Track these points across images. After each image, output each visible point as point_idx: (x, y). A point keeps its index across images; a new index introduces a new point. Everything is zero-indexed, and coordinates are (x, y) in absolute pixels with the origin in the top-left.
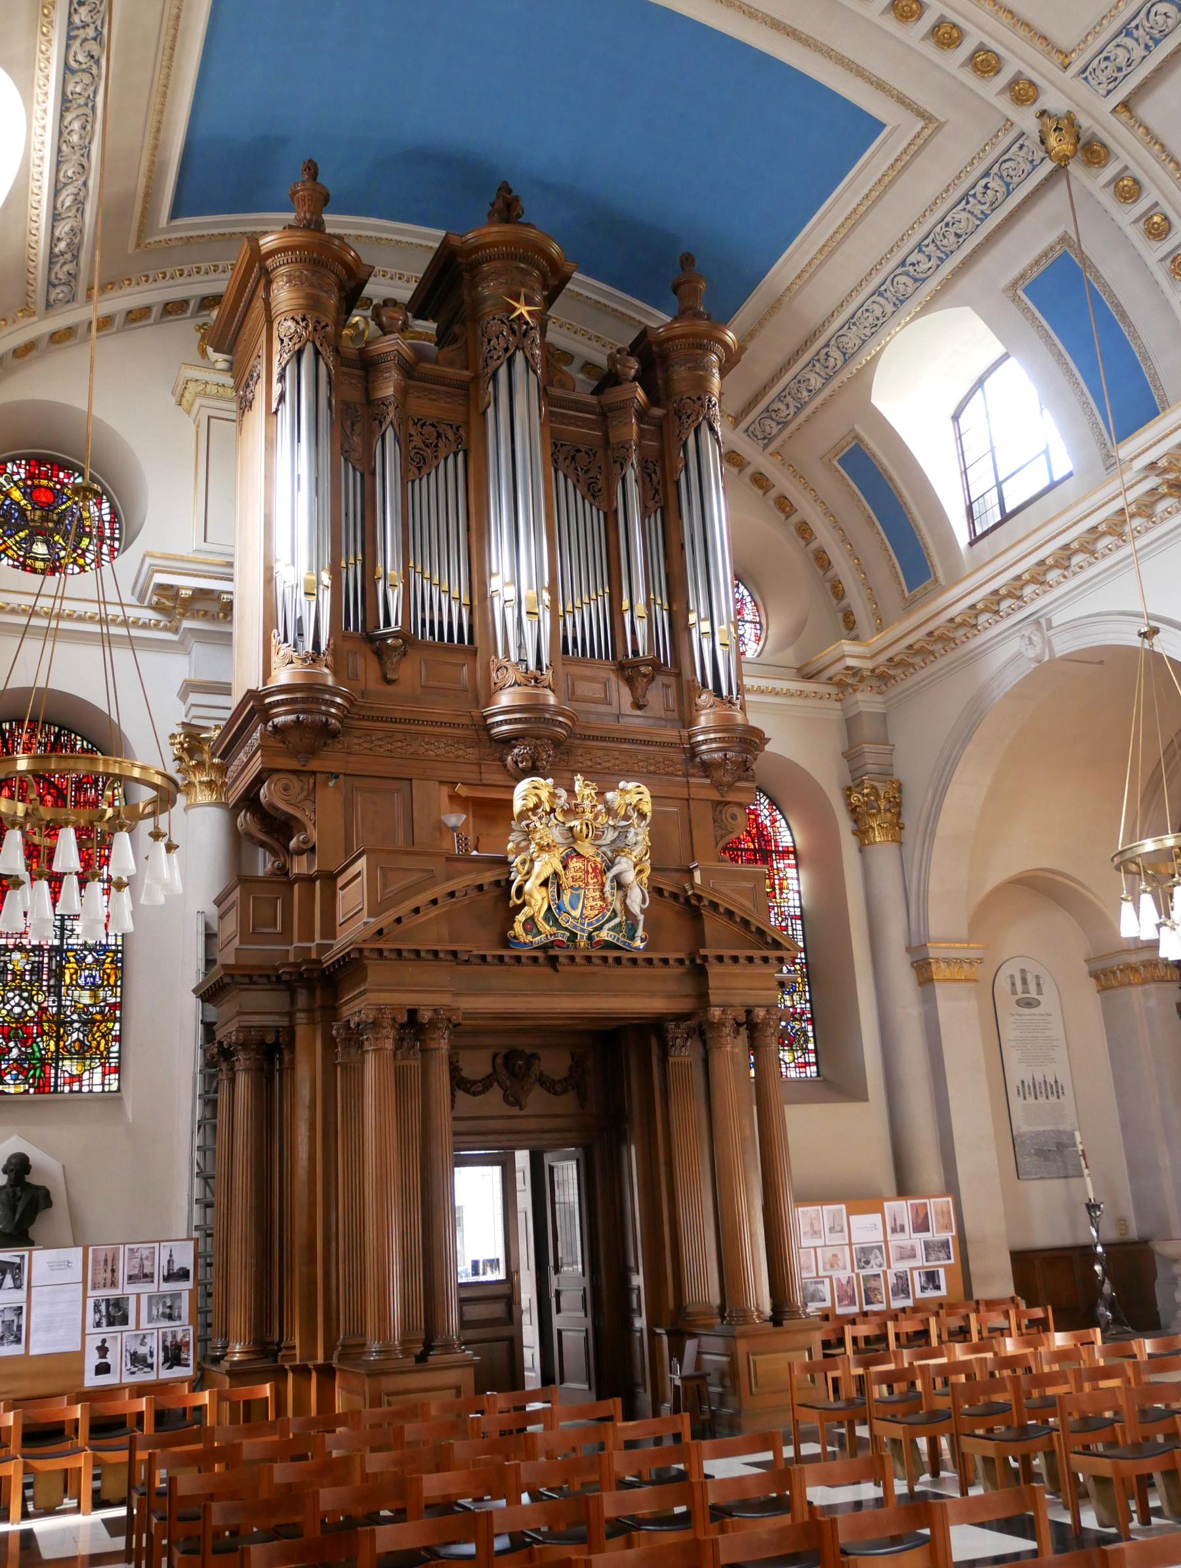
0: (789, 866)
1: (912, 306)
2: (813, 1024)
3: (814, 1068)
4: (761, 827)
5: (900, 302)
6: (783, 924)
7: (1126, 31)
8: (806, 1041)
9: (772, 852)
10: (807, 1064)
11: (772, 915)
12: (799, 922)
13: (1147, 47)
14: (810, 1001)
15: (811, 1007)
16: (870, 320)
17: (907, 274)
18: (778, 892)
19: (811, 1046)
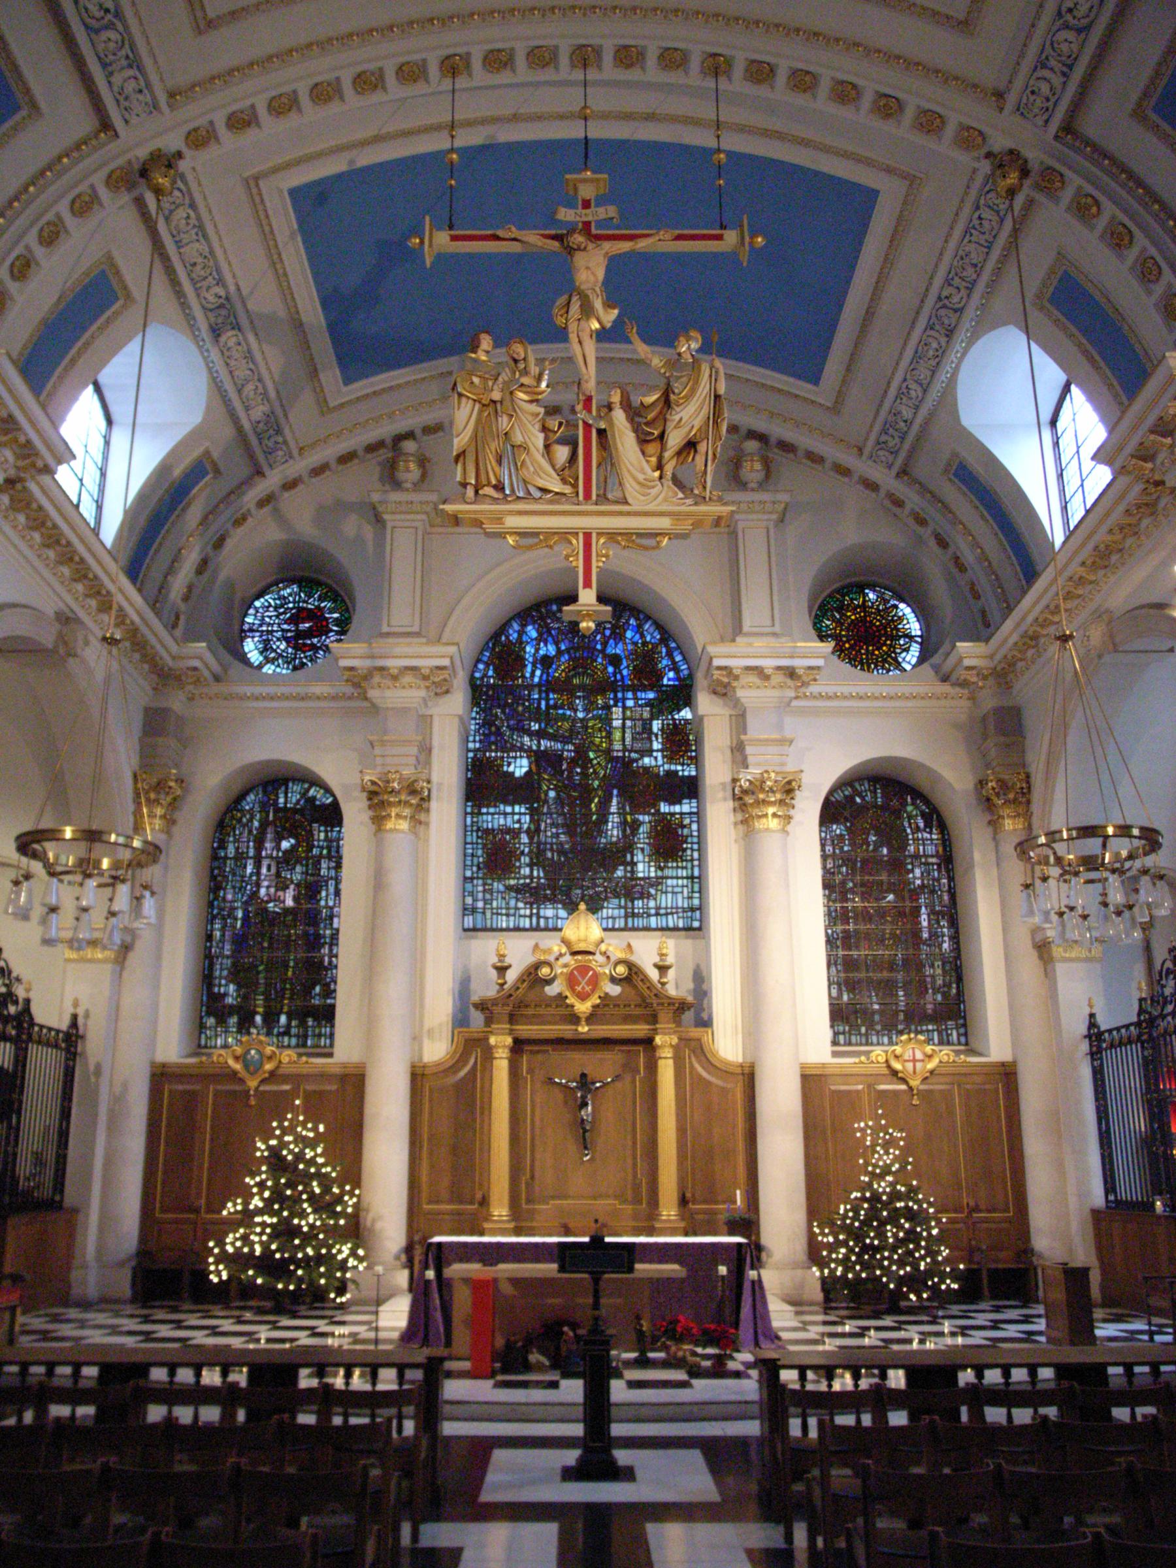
1: (961, 335)
5: (950, 333)
7: (1042, 64)
13: (1064, 74)
16: (931, 353)
17: (944, 306)
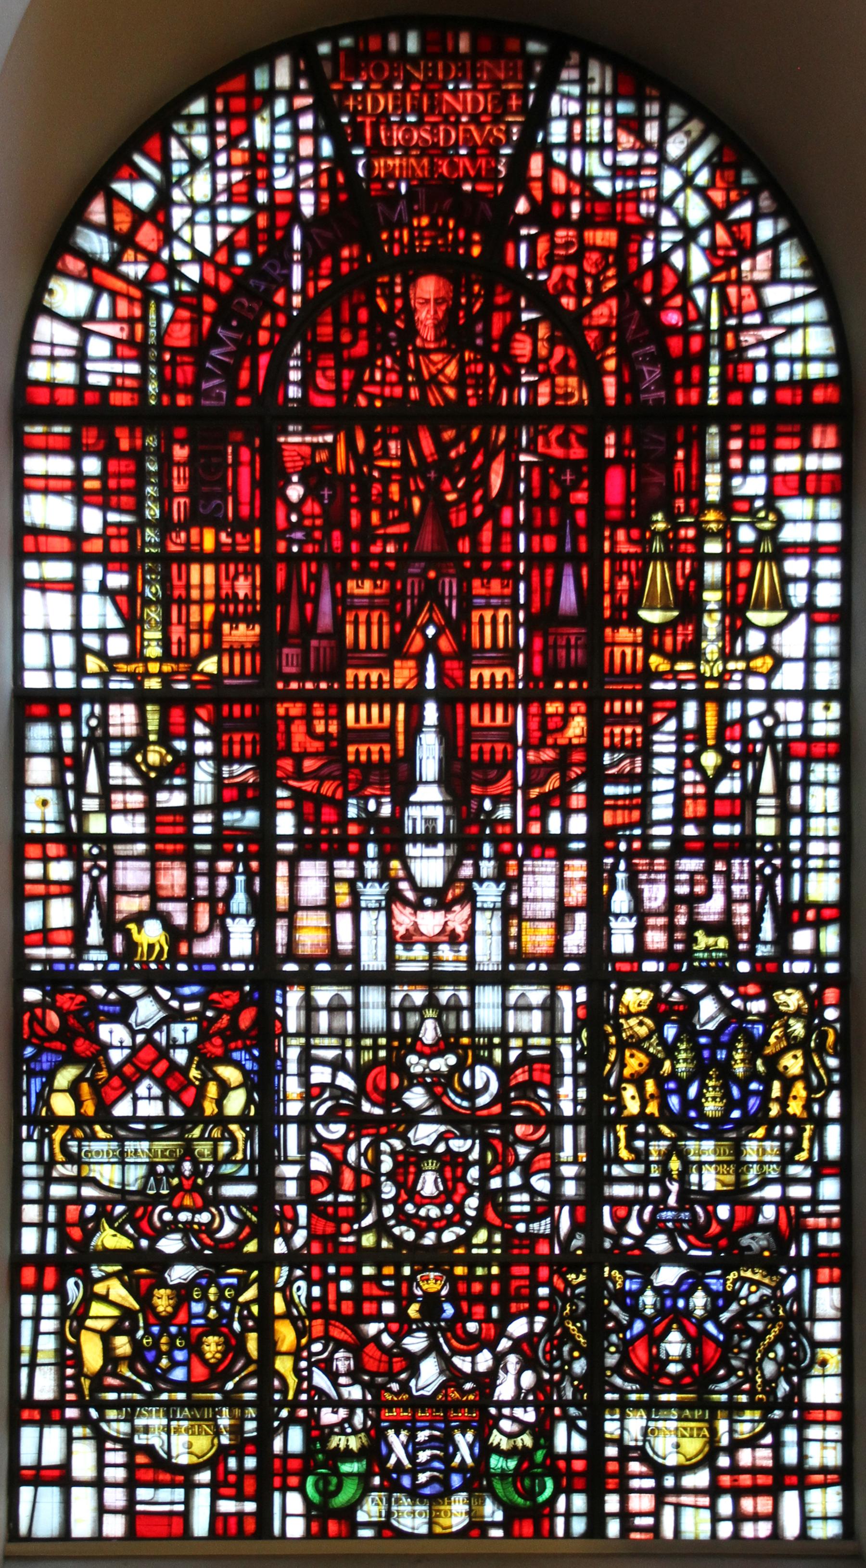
0: (805, 485)
2: (845, 1285)
3: (828, 1501)
4: (646, 291)
6: (729, 786)
8: (798, 1367)
9: (704, 415)
10: (801, 1478)
11: (664, 741)
12: (833, 772)
14: (842, 1168)
15: (845, 1199)
18: (712, 624)
19: (824, 1389)
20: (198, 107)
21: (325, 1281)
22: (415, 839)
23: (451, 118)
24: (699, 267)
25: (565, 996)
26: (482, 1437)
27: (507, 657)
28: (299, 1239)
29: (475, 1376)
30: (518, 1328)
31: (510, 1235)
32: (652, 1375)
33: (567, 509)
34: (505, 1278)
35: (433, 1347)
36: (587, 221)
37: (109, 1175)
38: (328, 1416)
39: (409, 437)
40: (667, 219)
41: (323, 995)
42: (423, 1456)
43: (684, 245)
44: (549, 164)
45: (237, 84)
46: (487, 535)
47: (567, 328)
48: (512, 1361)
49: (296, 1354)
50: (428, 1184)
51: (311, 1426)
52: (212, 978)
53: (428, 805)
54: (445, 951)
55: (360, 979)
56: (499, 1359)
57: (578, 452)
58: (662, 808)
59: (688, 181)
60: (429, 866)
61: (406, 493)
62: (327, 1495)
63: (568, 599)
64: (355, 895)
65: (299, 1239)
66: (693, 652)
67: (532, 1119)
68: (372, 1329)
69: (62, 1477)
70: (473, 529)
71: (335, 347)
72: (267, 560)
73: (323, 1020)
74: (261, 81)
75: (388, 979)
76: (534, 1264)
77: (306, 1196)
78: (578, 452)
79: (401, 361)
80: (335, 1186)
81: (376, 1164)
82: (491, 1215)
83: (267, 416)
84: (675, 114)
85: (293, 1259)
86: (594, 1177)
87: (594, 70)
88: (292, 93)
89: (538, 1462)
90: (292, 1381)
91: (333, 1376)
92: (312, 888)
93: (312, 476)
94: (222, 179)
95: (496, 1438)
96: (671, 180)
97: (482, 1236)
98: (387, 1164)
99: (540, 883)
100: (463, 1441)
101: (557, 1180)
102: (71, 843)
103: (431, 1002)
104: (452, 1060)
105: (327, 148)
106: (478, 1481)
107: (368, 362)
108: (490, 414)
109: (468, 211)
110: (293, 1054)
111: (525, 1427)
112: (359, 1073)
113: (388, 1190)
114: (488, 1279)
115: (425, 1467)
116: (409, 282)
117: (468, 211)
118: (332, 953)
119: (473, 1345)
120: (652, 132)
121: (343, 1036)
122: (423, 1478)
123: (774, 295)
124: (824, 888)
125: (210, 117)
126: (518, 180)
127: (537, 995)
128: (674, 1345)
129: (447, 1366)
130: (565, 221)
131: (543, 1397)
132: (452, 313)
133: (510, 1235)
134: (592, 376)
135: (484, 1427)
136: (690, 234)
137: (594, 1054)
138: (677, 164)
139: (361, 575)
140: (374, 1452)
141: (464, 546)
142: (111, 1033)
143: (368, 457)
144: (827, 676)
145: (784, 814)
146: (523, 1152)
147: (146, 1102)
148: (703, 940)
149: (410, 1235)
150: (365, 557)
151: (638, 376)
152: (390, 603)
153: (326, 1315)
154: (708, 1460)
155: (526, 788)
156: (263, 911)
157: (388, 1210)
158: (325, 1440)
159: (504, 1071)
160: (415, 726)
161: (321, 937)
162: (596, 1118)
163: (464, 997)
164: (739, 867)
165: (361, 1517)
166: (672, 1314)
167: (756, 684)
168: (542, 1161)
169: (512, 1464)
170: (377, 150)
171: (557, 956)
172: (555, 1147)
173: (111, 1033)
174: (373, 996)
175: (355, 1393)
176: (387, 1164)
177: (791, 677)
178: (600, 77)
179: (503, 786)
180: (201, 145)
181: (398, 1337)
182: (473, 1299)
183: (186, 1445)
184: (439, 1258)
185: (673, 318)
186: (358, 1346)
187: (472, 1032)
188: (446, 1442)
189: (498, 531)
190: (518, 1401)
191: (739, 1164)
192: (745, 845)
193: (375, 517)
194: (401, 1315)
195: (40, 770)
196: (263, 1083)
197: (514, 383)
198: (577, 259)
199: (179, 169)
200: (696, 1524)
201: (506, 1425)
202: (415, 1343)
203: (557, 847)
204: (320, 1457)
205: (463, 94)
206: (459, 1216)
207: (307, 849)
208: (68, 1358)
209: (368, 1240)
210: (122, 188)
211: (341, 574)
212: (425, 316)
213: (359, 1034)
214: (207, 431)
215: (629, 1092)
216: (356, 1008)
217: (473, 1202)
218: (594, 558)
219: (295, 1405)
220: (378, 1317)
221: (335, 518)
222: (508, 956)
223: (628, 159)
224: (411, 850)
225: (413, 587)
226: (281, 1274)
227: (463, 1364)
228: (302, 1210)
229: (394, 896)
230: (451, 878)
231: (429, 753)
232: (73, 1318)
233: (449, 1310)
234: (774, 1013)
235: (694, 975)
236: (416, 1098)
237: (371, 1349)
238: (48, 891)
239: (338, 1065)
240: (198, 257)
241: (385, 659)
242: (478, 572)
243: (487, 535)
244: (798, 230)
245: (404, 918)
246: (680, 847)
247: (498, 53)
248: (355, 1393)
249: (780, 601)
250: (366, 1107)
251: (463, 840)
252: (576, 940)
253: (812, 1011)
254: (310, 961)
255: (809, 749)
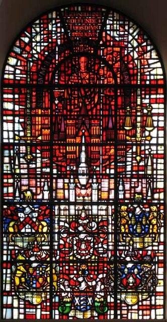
0: (157, 101)
2: (164, 267)
3: (160, 311)
4: (125, 60)
6: (142, 164)
8: (155, 284)
9: (137, 86)
10: (155, 307)
12: (162, 161)
14: (164, 243)
15: (164, 250)
18: (139, 130)
19: (160, 289)
20: (38, 22)
21: (62, 267)
22: (80, 174)
23: (87, 24)
24: (136, 56)
25: (110, 207)
26: (93, 299)
27: (98, 136)
28: (58, 258)
29: (92, 286)
30: (100, 276)
31: (99, 257)
32: (127, 286)
33: (110, 106)
34: (98, 266)
35: (84, 280)
36: (114, 46)
37: (20, 244)
38: (63, 294)
39: (79, 90)
40: (130, 46)
41: (62, 207)
42: (82, 303)
43: (133, 51)
44: (106, 34)
45: (45, 17)
46: (94, 111)
47: (110, 68)
48: (99, 283)
49: (57, 282)
50: (83, 246)
51: (60, 296)
52: (40, 203)
53: (83, 168)
54: (86, 198)
55: (70, 204)
56: (97, 283)
57: (112, 94)
58: (129, 168)
59: (134, 38)
60: (83, 180)
61: (78, 102)
62: (63, 311)
63: (110, 125)
64: (69, 186)
65: (58, 258)
66: (135, 136)
67: (103, 233)
68: (72, 276)
69: (11, 307)
70: (92, 110)
71: (65, 72)
72: (51, 116)
73: (62, 212)
74: (50, 16)
75: (75, 204)
76: (104, 262)
77: (59, 249)
78: (112, 94)
79: (78, 74)
80: (65, 247)
81: (73, 242)
82: (95, 253)
83: (52, 86)
84: (131, 24)
85: (57, 262)
86: (116, 245)
87: (115, 15)
88: (56, 19)
89: (104, 304)
90: (56, 287)
91: (64, 286)
92: (60, 185)
93: (61, 99)
94: (42, 37)
95: (96, 299)
96: (130, 38)
97: (93, 257)
98: (75, 242)
99: (105, 184)
100: (90, 299)
101: (108, 246)
102: (13, 175)
103: (84, 209)
104: (88, 221)
105: (63, 30)
106: (93, 308)
107: (71, 75)
108: (95, 86)
109: (90, 43)
110: (56, 219)
111: (102, 297)
112: (69, 223)
113: (75, 248)
114: (95, 266)
115: (82, 305)
116: (79, 58)
117: (90, 43)
118: (64, 198)
119: (92, 280)
120: (126, 28)
121: (66, 216)
122: (82, 307)
123: (150, 62)
124: (160, 185)
125: (40, 24)
126: (100, 38)
127: (104, 207)
128: (131, 280)
129: (87, 284)
130: (110, 46)
131: (105, 291)
132: (88, 64)
133: (99, 257)
134: (115, 77)
135: (94, 297)
136: (134, 49)
137: (115, 219)
138: (131, 34)
139: (69, 119)
140: (72, 302)
141: (90, 113)
142: (21, 215)
143: (70, 95)
144: (161, 141)
145: (153, 170)
146: (102, 240)
147: (27, 229)
148: (137, 196)
149: (79, 257)
150: (70, 115)
151: (124, 78)
152: (75, 125)
153: (63, 274)
154: (137, 303)
155: (102, 164)
156: (51, 190)
157: (75, 252)
158: (63, 299)
159: (98, 223)
160: (80, 151)
161: (62, 195)
162: (116, 232)
163: (90, 207)
164: (144, 181)
165: (70, 315)
166: (130, 273)
167: (147, 142)
168: (105, 242)
169: (99, 304)
170: (73, 31)
171: (108, 199)
172: (108, 239)
173: (21, 215)
174: (72, 207)
175: (69, 290)
176: (75, 242)
177: (154, 141)
178: (116, 16)
179: (98, 164)
180: (38, 30)
181: (77, 278)
182: (92, 270)
183: (36, 300)
184: (85, 262)
185: (131, 66)
186: (69, 280)
187: (92, 215)
188: (86, 300)
189: (97, 110)
190: (101, 291)
191: (144, 242)
192: (145, 176)
193: (72, 107)
194: (78, 274)
195: (6, 160)
196: (51, 225)
197: (99, 79)
198: (112, 54)
199: (34, 34)
200: (135, 316)
201: (98, 296)
202: (81, 279)
203: (108, 176)
204: (62, 303)
205: (90, 20)
206: (89, 253)
207: (59, 176)
208: (12, 282)
209: (71, 258)
210: (23, 38)
211: (66, 119)
212: (82, 65)
213: (69, 215)
214: (39, 89)
215: (122, 227)
216: (69, 210)
217: (92, 250)
218: (116, 116)
219: (57, 292)
220: (73, 274)
221: (65, 108)
222: (98, 199)
223: (122, 33)
224: (80, 177)
225: (80, 122)
226: (54, 265)
227: (90, 284)
228: (58, 252)
229: (76, 186)
230: (88, 183)
231: (83, 156)
232: (13, 274)
233: (87, 272)
234: (151, 211)
235: (135, 203)
236: (81, 229)
237: (72, 280)
238: (8, 185)
239: (65, 222)
240: (38, 53)
241: (75, 137)
242: (92, 119)
243: (94, 111)
244: (156, 48)
245: (78, 191)
246: (132, 177)
247: (96, 11)
248: (69, 290)
249: (152, 126)
250: (71, 230)
251: (90, 175)
252: (112, 196)
253: (158, 211)
254: (60, 200)
255: (157, 156)
